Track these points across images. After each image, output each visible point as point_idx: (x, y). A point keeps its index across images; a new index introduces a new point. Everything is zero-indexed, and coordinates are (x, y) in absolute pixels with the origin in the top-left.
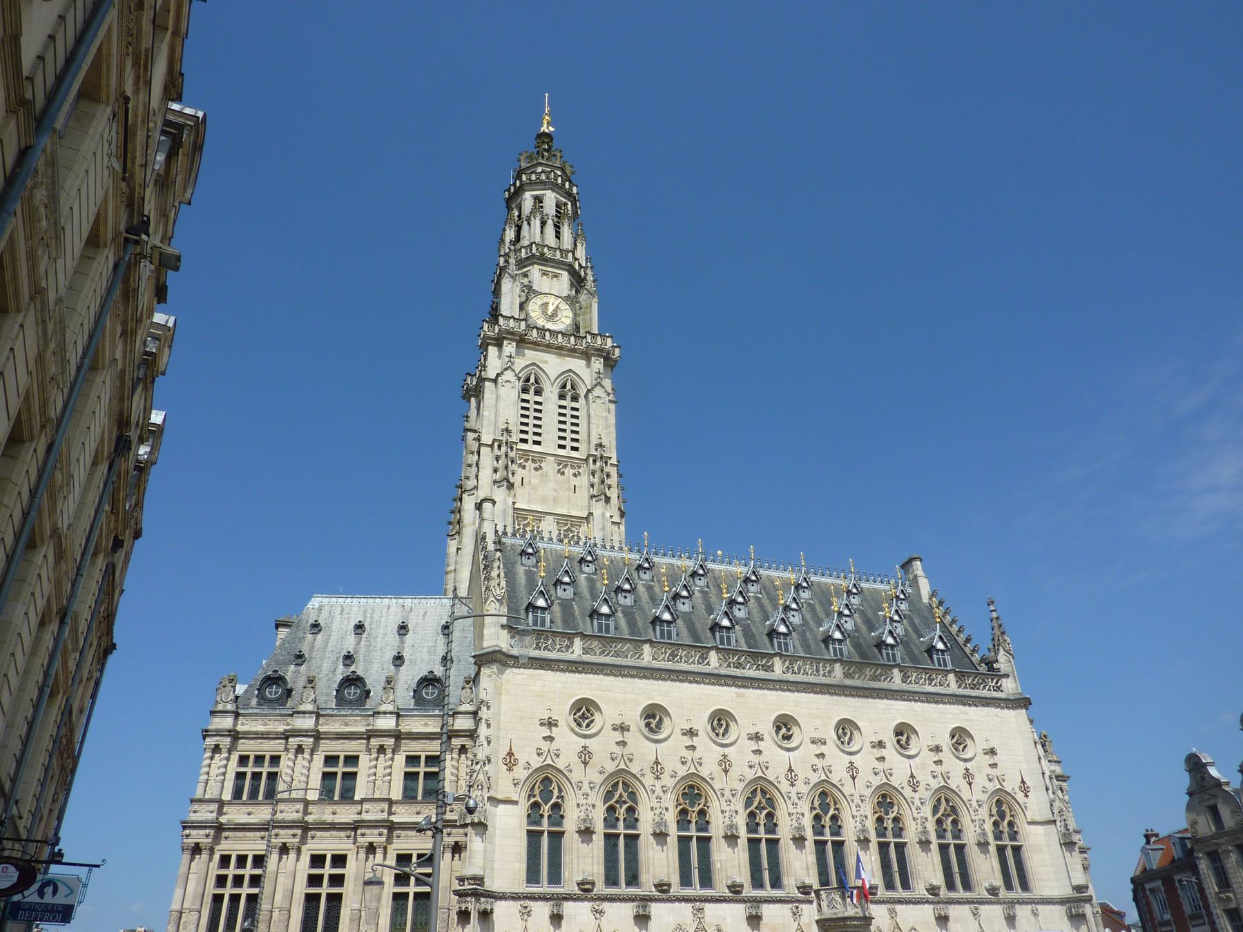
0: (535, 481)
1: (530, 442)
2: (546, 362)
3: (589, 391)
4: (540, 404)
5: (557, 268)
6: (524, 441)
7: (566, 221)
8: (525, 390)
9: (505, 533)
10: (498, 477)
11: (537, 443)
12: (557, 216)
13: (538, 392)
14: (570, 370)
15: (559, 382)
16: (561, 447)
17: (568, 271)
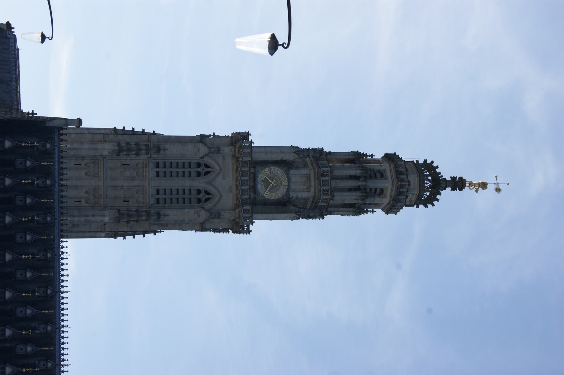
0: (127, 173)
1: (158, 170)
2: (224, 178)
3: (203, 208)
4: (190, 176)
5: (315, 187)
6: (157, 165)
7: (361, 194)
8: (199, 165)
9: (62, 134)
10: (123, 145)
11: (158, 175)
12: (371, 189)
13: (199, 174)
14: (221, 196)
15: (210, 188)
16: (158, 192)
17: (314, 197)
